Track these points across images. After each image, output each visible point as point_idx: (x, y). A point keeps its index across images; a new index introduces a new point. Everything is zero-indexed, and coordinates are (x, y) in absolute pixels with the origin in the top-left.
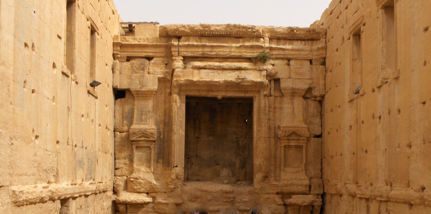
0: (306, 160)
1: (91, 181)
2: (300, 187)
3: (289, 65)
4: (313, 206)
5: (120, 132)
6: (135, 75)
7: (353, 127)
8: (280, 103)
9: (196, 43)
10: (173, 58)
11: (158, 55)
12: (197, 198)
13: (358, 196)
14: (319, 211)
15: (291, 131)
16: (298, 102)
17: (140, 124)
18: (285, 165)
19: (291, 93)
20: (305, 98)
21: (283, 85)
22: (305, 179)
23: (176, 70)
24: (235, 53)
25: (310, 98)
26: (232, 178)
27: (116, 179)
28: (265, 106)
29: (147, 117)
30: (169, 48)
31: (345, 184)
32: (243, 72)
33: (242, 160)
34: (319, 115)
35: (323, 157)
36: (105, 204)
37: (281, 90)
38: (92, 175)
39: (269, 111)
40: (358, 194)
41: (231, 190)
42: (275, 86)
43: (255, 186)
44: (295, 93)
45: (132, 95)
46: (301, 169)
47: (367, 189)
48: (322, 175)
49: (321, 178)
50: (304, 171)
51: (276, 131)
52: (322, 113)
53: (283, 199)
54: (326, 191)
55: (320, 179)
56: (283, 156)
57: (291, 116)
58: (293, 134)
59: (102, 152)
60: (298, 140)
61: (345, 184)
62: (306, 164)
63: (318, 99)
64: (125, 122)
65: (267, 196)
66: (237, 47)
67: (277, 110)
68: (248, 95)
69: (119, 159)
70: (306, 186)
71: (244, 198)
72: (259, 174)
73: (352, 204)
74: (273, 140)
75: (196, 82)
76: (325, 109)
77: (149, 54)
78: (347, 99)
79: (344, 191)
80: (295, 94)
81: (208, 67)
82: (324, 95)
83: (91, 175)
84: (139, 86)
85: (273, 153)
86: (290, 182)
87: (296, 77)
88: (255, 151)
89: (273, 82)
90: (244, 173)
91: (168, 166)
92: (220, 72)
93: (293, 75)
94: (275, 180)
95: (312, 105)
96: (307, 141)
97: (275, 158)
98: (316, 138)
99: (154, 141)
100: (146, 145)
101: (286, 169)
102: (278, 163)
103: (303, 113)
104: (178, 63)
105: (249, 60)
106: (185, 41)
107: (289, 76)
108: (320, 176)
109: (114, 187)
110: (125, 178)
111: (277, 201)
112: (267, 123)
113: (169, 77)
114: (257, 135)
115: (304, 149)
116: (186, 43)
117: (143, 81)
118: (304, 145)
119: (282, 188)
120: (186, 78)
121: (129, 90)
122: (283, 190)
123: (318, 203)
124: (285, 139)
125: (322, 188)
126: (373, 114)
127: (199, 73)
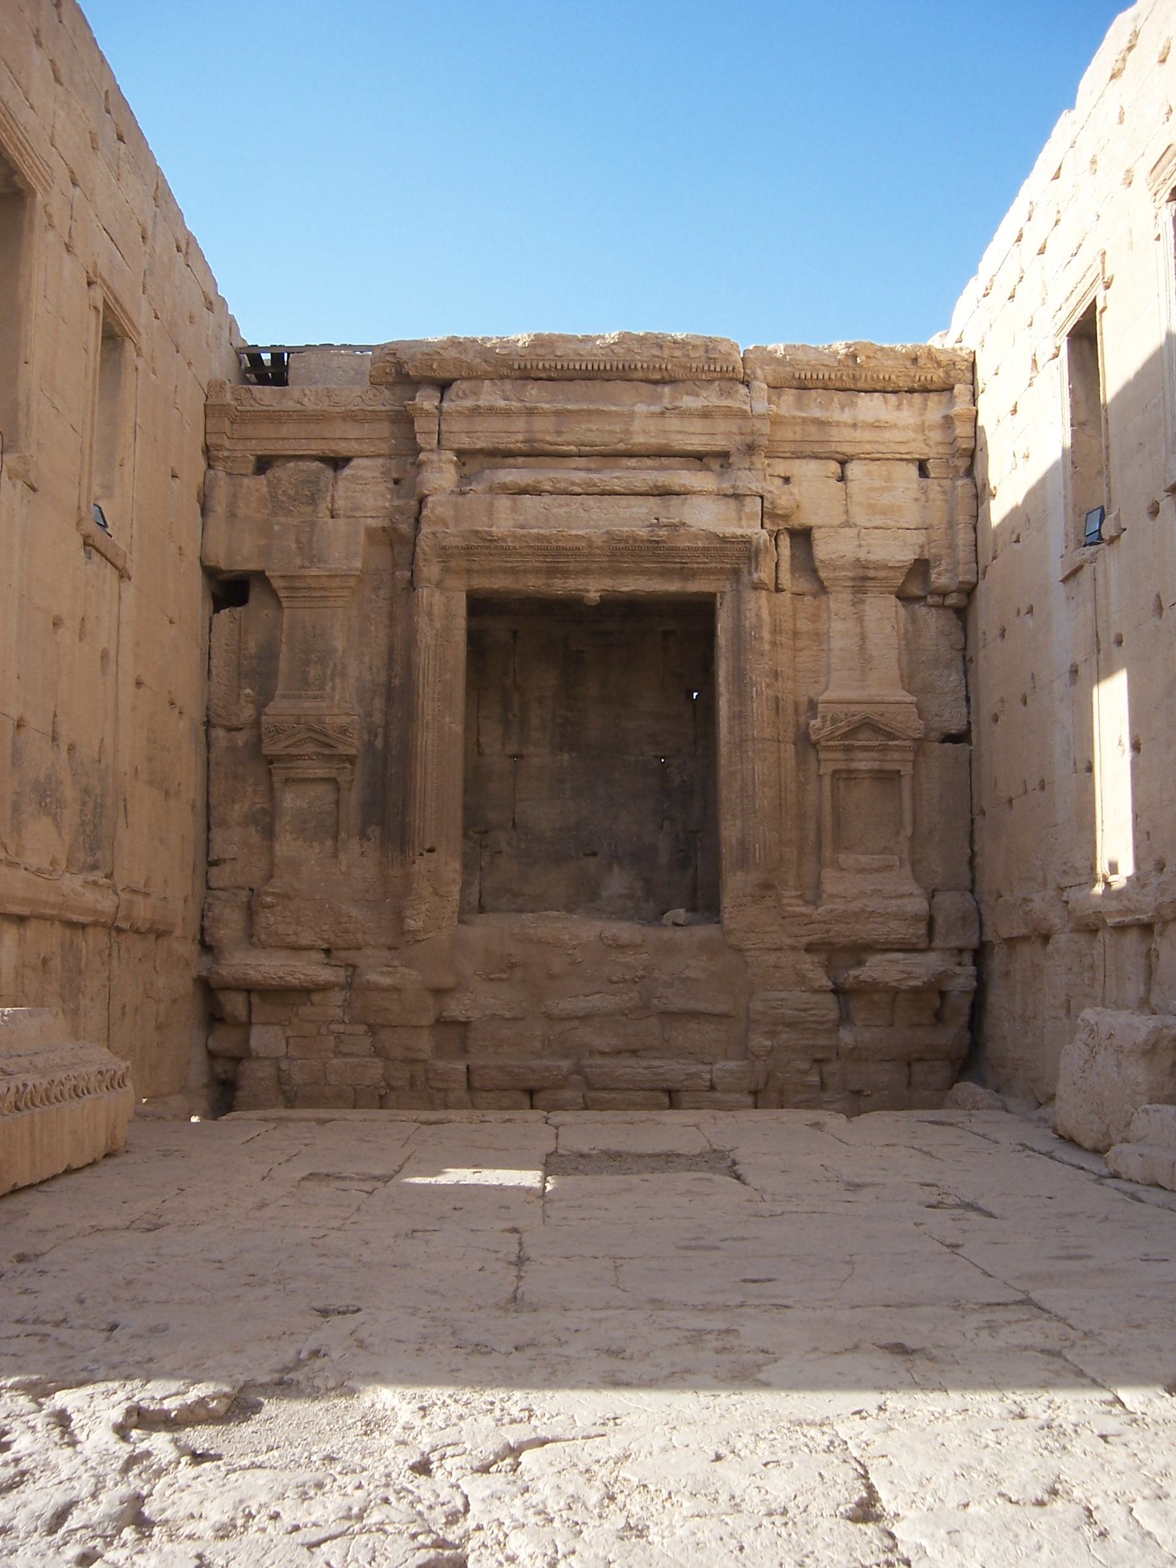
0: (915, 821)
1: (98, 876)
2: (893, 924)
3: (842, 478)
4: (943, 994)
5: (229, 729)
6: (282, 519)
7: (1081, 669)
8: (815, 618)
9: (502, 403)
10: (422, 456)
11: (367, 448)
12: (512, 966)
13: (1110, 921)
14: (966, 1011)
16: (883, 614)
17: (300, 696)
18: (839, 845)
19: (854, 579)
20: (904, 598)
21: (823, 549)
22: (911, 894)
23: (430, 499)
24: (644, 433)
27: (210, 900)
30: (404, 419)
31: (1062, 889)
32: (675, 501)
34: (960, 658)
35: (976, 810)
36: (160, 982)
37: (815, 571)
38: (99, 855)
39: (773, 644)
40: (1110, 914)
41: (638, 939)
42: (793, 556)
43: (726, 922)
44: (865, 578)
45: (273, 593)
46: (896, 858)
47: (1144, 886)
48: (973, 881)
50: (908, 867)
52: (969, 654)
53: (829, 968)
54: (989, 936)
55: (968, 895)
56: (827, 808)
57: (857, 659)
58: (868, 727)
59: (150, 782)
60: (884, 749)
61: (1062, 889)
62: (911, 839)
63: (952, 600)
64: (248, 691)
65: (772, 958)
66: (653, 415)
67: (800, 644)
69: (223, 823)
70: (916, 918)
71: (688, 966)
72: (740, 875)
73: (1088, 961)
75: (502, 539)
76: (980, 634)
77: (333, 446)
78: (1058, 570)
79: (1056, 919)
80: (869, 583)
81: (547, 486)
83: (94, 847)
86: (855, 906)
88: (724, 792)
90: (687, 875)
91: (402, 851)
92: (591, 501)
94: (801, 897)
96: (916, 754)
98: (947, 745)
99: (351, 759)
100: (320, 773)
103: (899, 654)
104: (440, 476)
105: (698, 458)
106: (465, 396)
107: (843, 518)
108: (968, 883)
109: (202, 930)
110: (243, 896)
111: (811, 975)
113: (405, 528)
114: (731, 732)
116: (469, 403)
117: (310, 542)
118: (907, 770)
119: (827, 926)
120: (465, 526)
121: (261, 576)
123: (961, 980)
125: (977, 925)
126: (1158, 596)
127: (514, 510)
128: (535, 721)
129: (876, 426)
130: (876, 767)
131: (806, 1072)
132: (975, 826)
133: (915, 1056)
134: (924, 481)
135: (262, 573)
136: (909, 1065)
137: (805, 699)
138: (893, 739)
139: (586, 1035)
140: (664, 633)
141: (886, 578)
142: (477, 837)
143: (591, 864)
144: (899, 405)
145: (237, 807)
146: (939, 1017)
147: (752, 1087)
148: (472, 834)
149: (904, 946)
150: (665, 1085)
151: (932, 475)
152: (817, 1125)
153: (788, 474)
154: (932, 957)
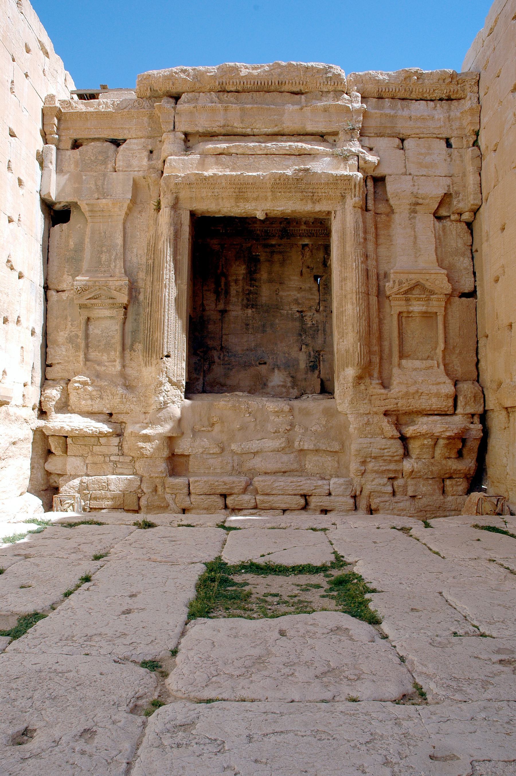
2: (434, 400)
10: (164, 136)
15: (414, 282)
17: (96, 271)
25: (449, 216)
26: (291, 390)
28: (356, 229)
29: (110, 257)
33: (312, 353)
37: (387, 200)
39: (365, 239)
42: (375, 192)
44: (417, 204)
46: (436, 362)
49: (478, 381)
50: (442, 367)
51: (381, 283)
53: (398, 425)
56: (395, 334)
60: (429, 300)
62: (444, 351)
63: (466, 216)
68: (318, 208)
70: (447, 396)
74: (374, 300)
76: (484, 234)
80: (418, 208)
82: (480, 206)
84: (96, 196)
85: (375, 326)
87: (419, 174)
89: (370, 183)
93: (413, 169)
95: (455, 232)
97: (380, 338)
98: (463, 299)
101: (404, 362)
102: (387, 351)
103: (436, 247)
105: (321, 137)
108: (475, 376)
109: (40, 402)
112: (362, 263)
115: (440, 319)
122: (399, 405)
124: (400, 300)
125: (482, 401)
128: (233, 292)
129: (423, 119)
130: (423, 310)
131: (384, 485)
132: (479, 345)
133: (447, 476)
134: (449, 150)
135: (76, 203)
136: (443, 481)
137: (383, 272)
138: (433, 294)
139: (257, 463)
140: (304, 246)
141: (428, 204)
142: (201, 354)
143: (263, 369)
144: (436, 107)
145: (62, 333)
146: (460, 455)
147: (353, 494)
148: (199, 352)
149: (440, 412)
150: (302, 492)
151: (454, 146)
152: (405, 530)
153: (372, 146)
154: (457, 419)
